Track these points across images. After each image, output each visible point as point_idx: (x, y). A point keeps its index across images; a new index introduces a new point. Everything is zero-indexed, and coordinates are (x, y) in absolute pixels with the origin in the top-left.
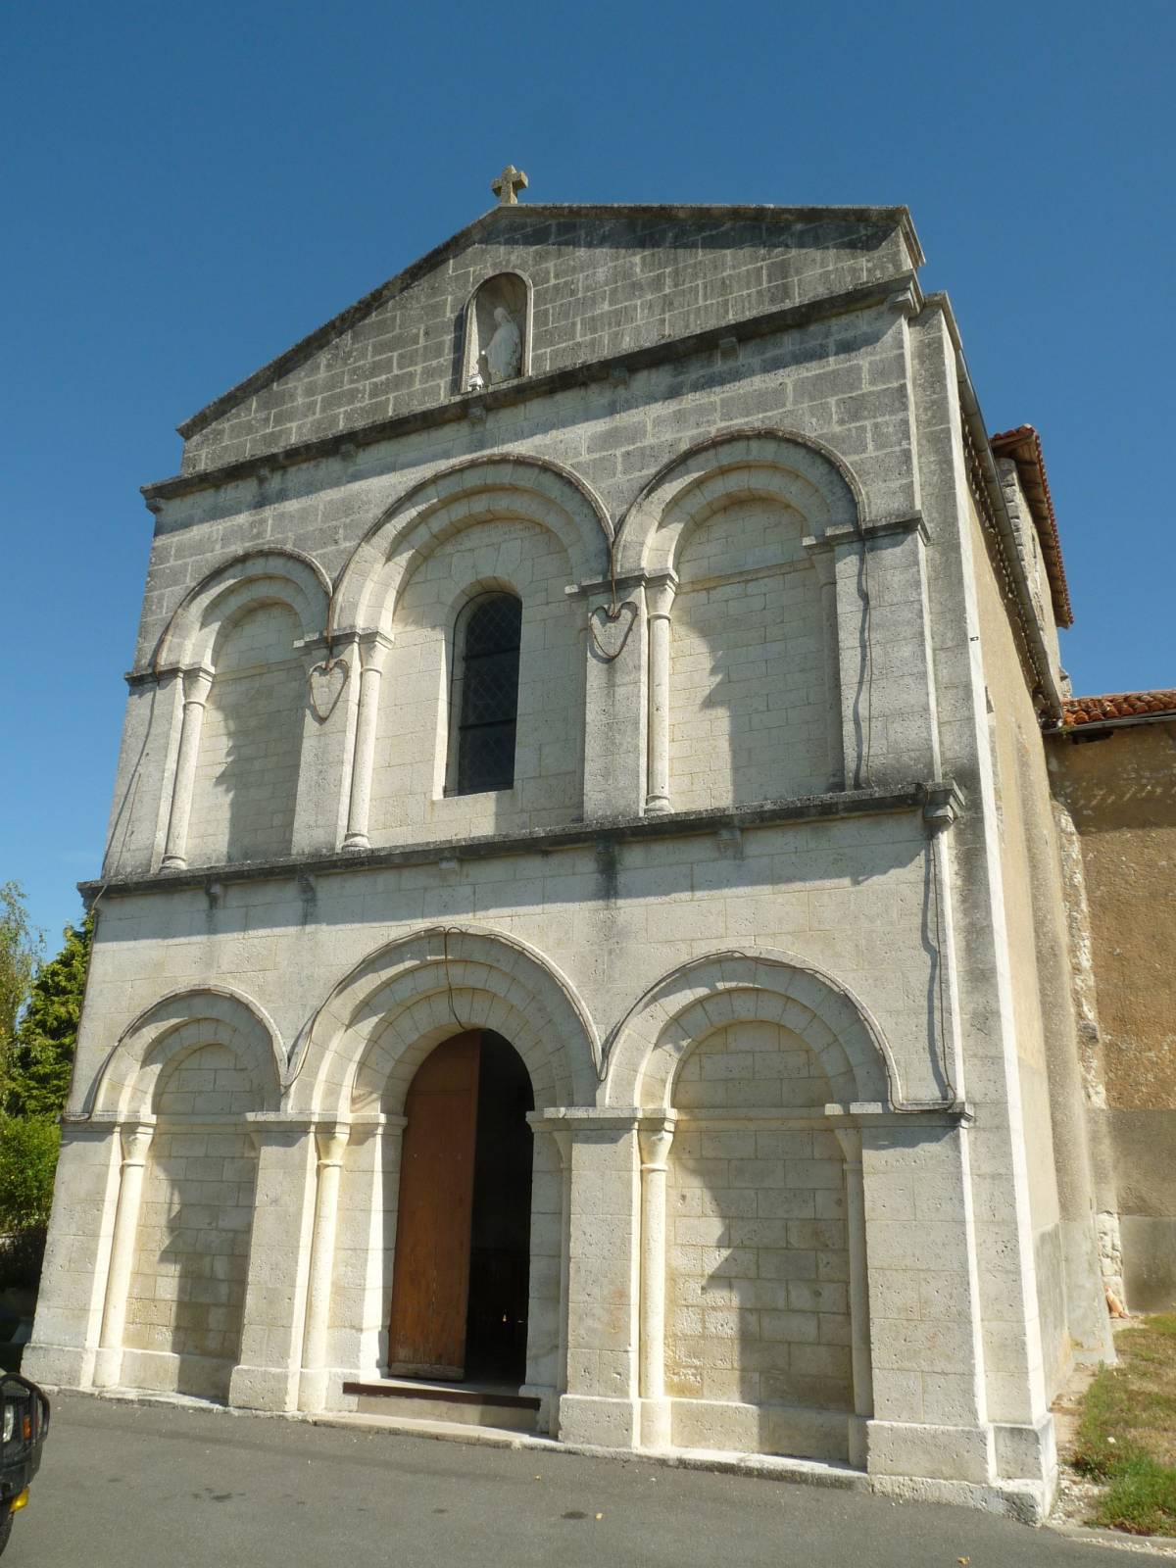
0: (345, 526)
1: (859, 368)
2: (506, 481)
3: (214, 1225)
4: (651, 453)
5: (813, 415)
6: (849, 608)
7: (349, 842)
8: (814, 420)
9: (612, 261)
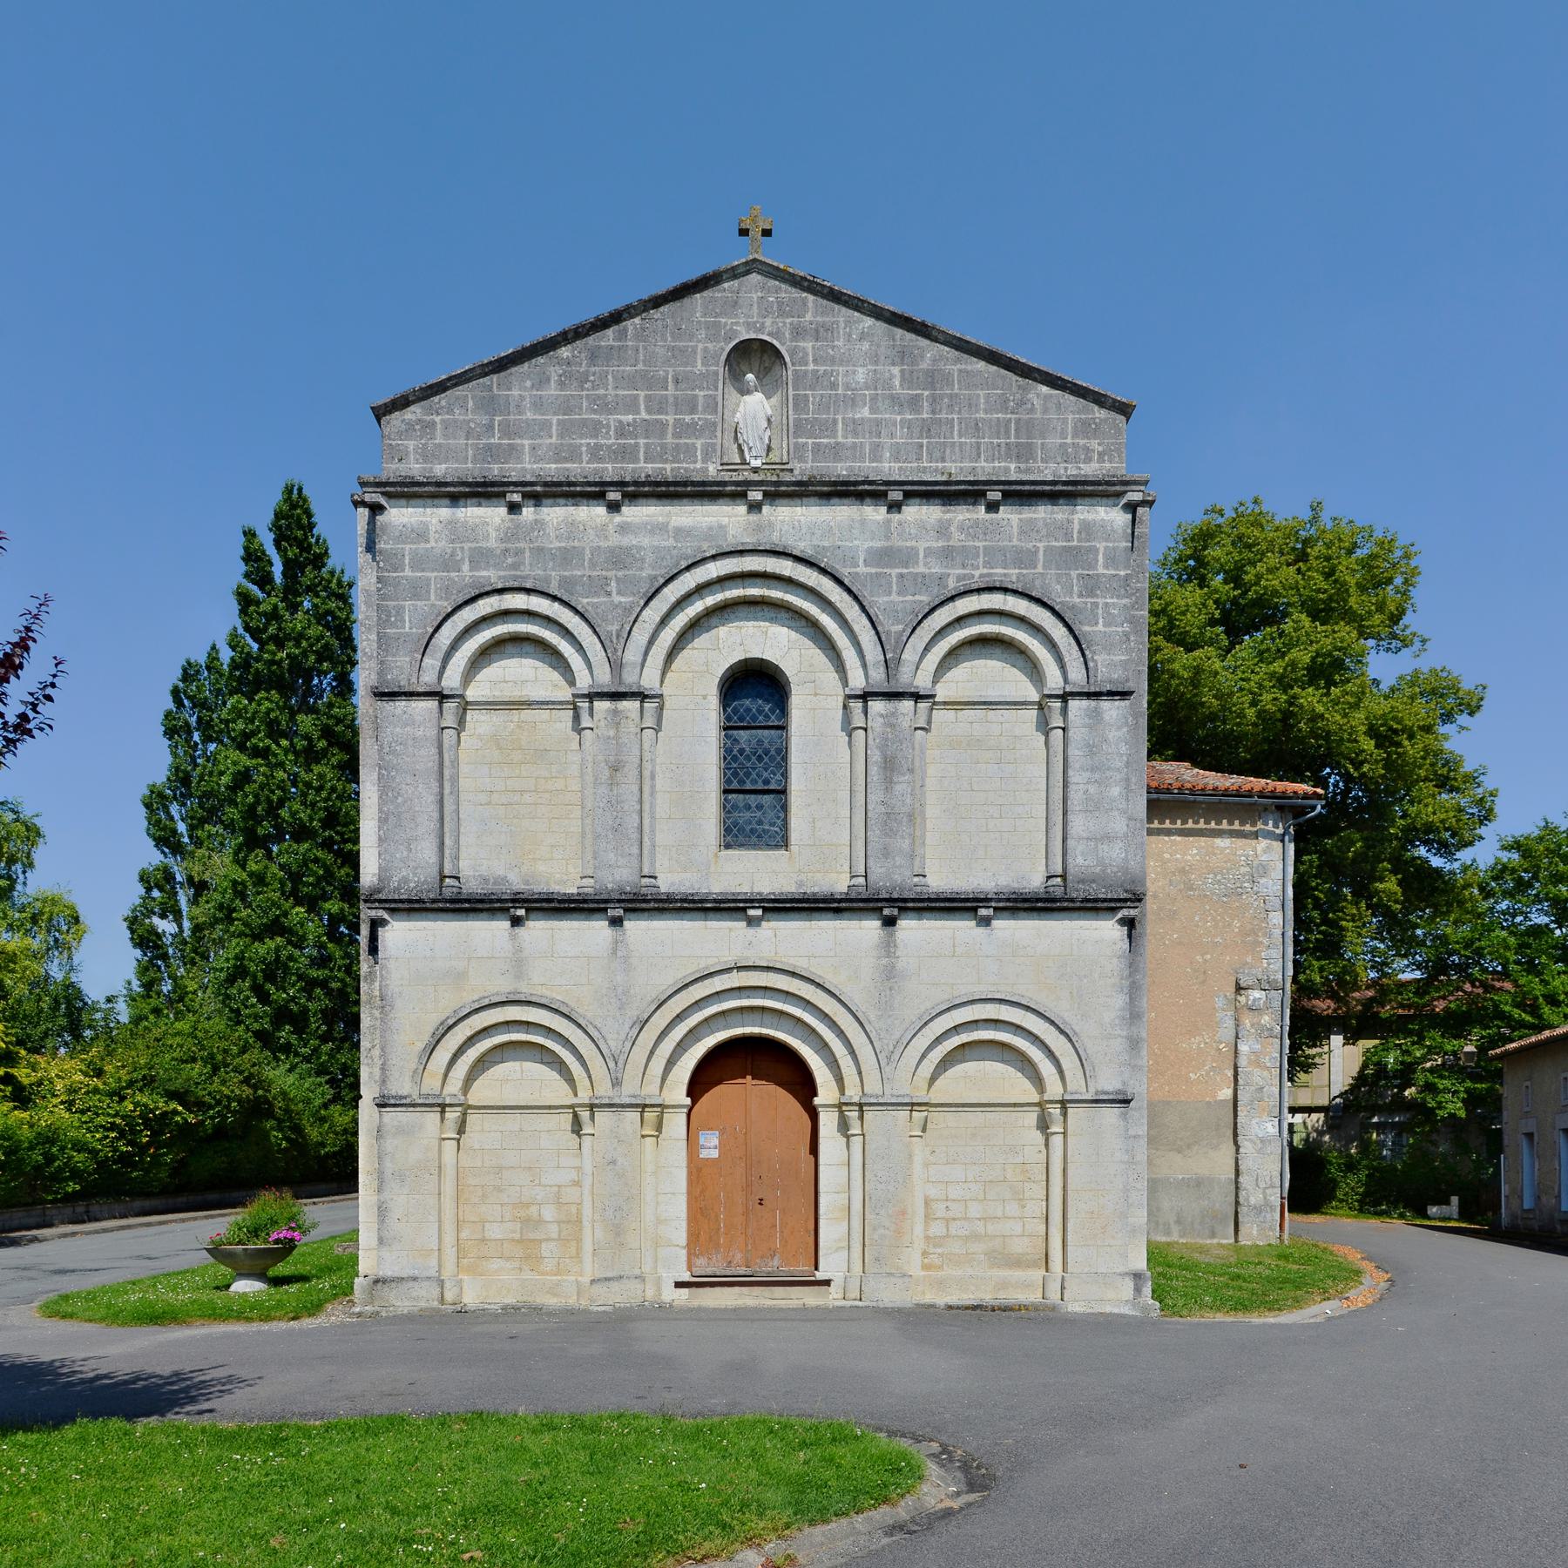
0: (618, 580)
1: (1097, 550)
2: (787, 573)
3: (537, 1182)
4: (922, 581)
5: (1059, 583)
6: (1077, 752)
7: (1049, 883)
8: (1059, 587)
9: (871, 364)
